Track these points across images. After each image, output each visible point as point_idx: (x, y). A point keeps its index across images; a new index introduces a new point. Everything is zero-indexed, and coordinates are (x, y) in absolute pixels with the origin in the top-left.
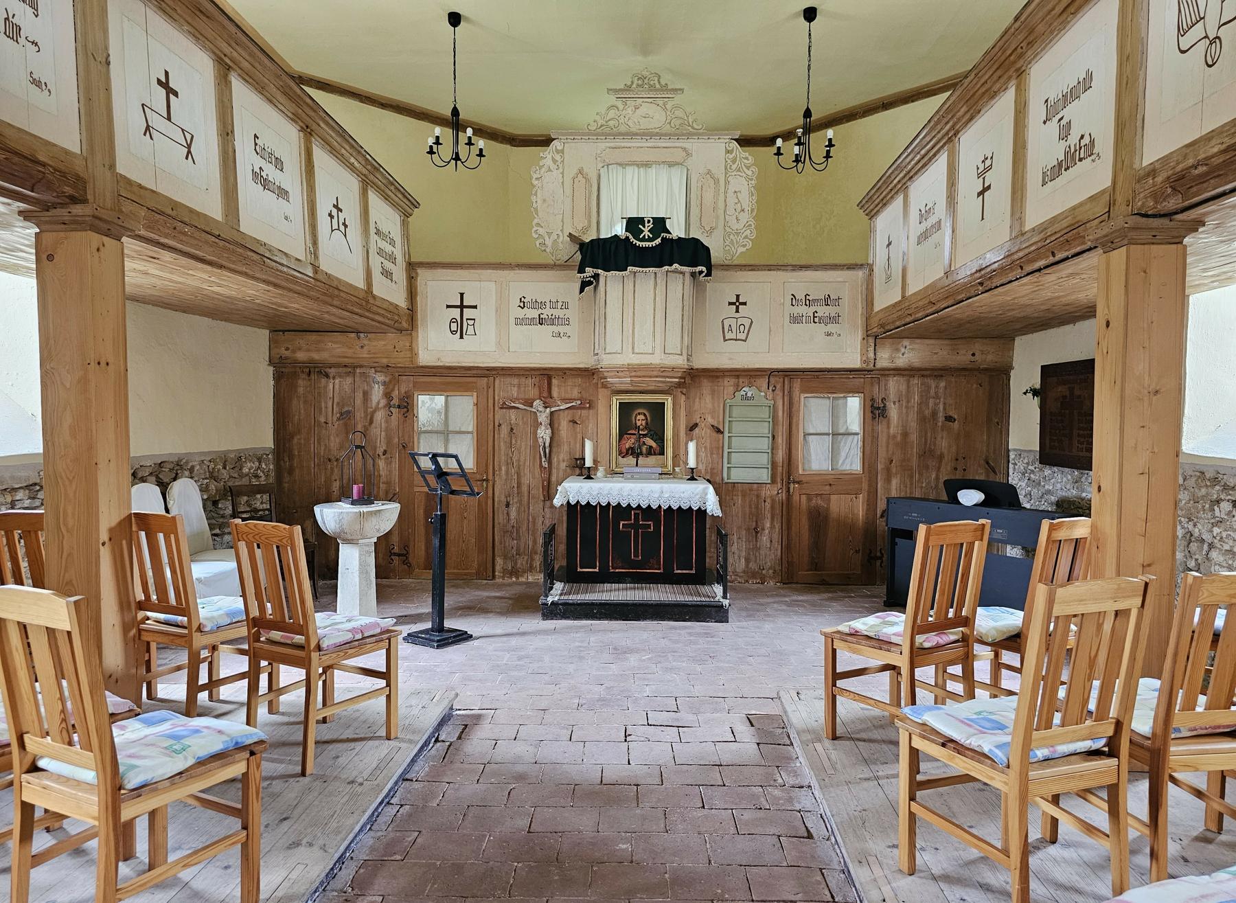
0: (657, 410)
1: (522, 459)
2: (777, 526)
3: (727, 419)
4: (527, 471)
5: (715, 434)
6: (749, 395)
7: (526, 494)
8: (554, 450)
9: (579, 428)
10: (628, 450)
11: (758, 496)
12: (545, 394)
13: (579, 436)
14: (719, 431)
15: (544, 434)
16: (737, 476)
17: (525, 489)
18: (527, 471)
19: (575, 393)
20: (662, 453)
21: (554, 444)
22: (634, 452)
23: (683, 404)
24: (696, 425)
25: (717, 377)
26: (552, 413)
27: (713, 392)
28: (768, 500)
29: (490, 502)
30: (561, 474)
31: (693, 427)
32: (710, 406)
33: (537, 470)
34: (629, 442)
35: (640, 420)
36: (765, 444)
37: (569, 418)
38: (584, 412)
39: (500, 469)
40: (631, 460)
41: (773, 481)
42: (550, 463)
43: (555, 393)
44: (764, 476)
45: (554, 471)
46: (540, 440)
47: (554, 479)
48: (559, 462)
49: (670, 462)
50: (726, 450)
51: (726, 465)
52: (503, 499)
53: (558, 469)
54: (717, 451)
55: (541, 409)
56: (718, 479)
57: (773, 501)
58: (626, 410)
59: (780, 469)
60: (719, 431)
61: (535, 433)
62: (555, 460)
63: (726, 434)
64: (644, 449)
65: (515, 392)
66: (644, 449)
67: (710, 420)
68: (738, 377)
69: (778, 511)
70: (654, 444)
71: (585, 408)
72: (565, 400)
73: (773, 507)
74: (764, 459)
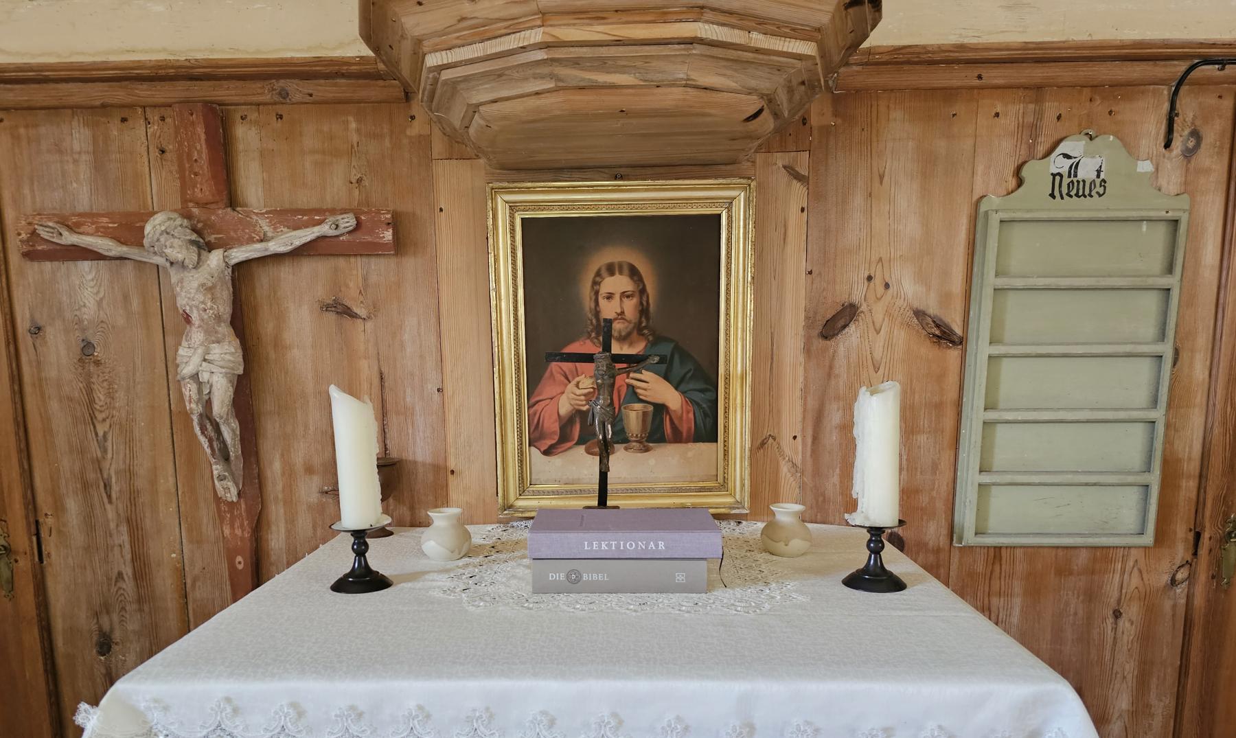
0: (689, 247)
1: (142, 467)
2: (1161, 705)
3: (989, 280)
4: (167, 512)
5: (926, 350)
6: (1086, 172)
8: (271, 428)
9: (362, 335)
10: (566, 424)
11: (1091, 595)
12: (204, 189)
14: (944, 336)
15: (208, 363)
16: (1014, 514)
17: (164, 583)
18: (167, 512)
19: (336, 185)
20: (707, 430)
22: (596, 433)
23: (795, 219)
24: (848, 314)
25: (949, 94)
27: (927, 165)
28: (1133, 611)
29: (32, 637)
31: (833, 323)
32: (911, 227)
33: (206, 514)
34: (573, 391)
35: (613, 295)
36: (1132, 384)
38: (378, 269)
39: (59, 508)
40: (581, 465)
41: (1162, 535)
43: (253, 184)
44: (1121, 516)
45: (276, 512)
46: (190, 390)
48: (289, 472)
49: (739, 471)
50: (974, 415)
51: (970, 477)
52: (83, 619)
54: (933, 427)
55: (178, 250)
56: (933, 532)
57: (1151, 612)
58: (552, 250)
59: (1188, 487)
60: (944, 336)
62: (274, 468)
63: (980, 349)
64: (633, 418)
65: (83, 196)
66: (633, 418)
67: (910, 289)
68: (1037, 91)
69: (1168, 652)
70: (670, 397)
71: (373, 250)
72: (288, 216)
73: (1146, 638)
74: (1129, 446)
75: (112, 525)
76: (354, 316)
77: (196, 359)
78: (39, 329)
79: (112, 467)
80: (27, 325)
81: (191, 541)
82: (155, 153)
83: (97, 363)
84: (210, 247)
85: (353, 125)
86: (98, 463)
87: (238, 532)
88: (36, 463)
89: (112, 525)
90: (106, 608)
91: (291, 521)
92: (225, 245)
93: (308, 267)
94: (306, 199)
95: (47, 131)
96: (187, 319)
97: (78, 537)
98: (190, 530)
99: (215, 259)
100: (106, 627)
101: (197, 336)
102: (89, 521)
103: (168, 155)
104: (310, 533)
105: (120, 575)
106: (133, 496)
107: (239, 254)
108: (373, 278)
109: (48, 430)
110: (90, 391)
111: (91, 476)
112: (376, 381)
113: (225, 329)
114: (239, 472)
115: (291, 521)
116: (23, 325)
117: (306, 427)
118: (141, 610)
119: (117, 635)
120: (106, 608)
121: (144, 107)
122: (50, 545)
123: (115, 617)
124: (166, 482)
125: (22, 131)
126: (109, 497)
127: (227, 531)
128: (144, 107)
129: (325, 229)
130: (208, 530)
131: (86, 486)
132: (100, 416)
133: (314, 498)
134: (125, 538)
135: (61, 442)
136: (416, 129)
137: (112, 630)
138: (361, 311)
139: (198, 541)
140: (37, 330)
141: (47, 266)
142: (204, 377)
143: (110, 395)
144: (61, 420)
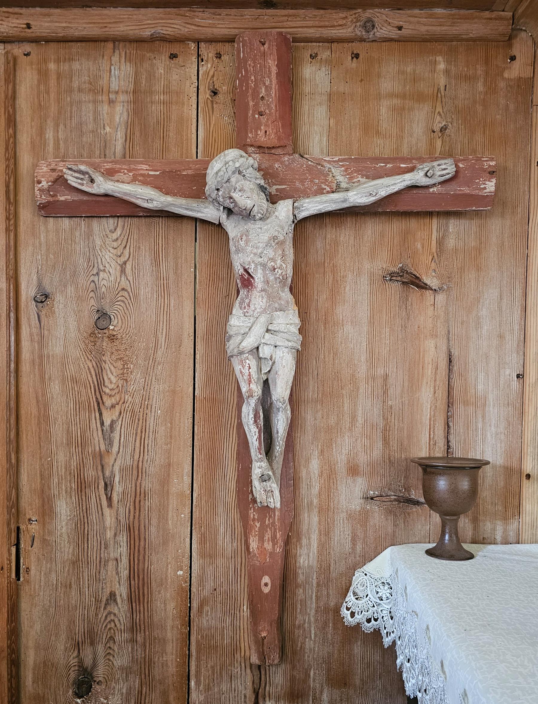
7: (171, 633)
8: (310, 417)
9: (428, 310)
12: (266, 132)
13: (433, 351)
17: (166, 607)
18: (177, 520)
21: (311, 391)
26: (302, 226)
30: (342, 535)
37: (383, 263)
39: (47, 511)
42: (290, 482)
45: (310, 521)
46: (246, 372)
47: (307, 557)
48: (329, 475)
52: (62, 654)
53: (326, 510)
55: (248, 196)
61: (219, 334)
62: (312, 468)
72: (367, 167)
75: (109, 534)
76: (424, 287)
77: (258, 329)
78: (47, 296)
79: (116, 464)
80: (32, 292)
81: (202, 555)
82: (205, 94)
83: (112, 338)
84: (273, 200)
85: (442, 66)
86: (101, 456)
87: (268, 546)
88: (25, 457)
89: (109, 534)
90: (91, 638)
91: (326, 533)
92: (294, 195)
93: (371, 229)
94: (380, 147)
95: (82, 67)
96: (247, 281)
97: (66, 550)
98: (203, 541)
99: (284, 210)
100: (88, 662)
101: (258, 300)
102: (81, 530)
103: (220, 97)
104: (348, 546)
105: (112, 596)
106: (138, 498)
107: (311, 206)
108: (451, 243)
109: (44, 417)
110: (100, 371)
111: (90, 473)
112: (443, 364)
113: (286, 295)
114: (279, 472)
115: (326, 533)
116: (28, 291)
117: (354, 418)
118: (133, 641)
119: (100, 673)
120: (91, 638)
121: (198, 42)
122: (31, 558)
123: (100, 649)
124: (180, 483)
125: (52, 66)
126: (109, 499)
127: (254, 544)
128: (198, 42)
129: (417, 177)
130: (226, 541)
131: (82, 486)
132: (108, 402)
133: (357, 504)
134: (124, 550)
135: (58, 432)
136: (516, 70)
137: (95, 665)
138: (431, 281)
139: (210, 555)
140: (43, 298)
141: (66, 223)
142: (265, 352)
143: (124, 377)
144: (60, 403)
